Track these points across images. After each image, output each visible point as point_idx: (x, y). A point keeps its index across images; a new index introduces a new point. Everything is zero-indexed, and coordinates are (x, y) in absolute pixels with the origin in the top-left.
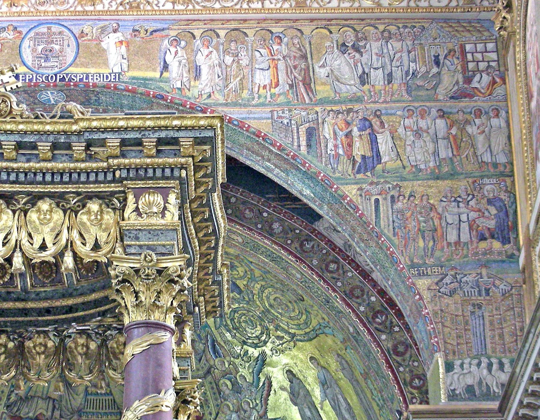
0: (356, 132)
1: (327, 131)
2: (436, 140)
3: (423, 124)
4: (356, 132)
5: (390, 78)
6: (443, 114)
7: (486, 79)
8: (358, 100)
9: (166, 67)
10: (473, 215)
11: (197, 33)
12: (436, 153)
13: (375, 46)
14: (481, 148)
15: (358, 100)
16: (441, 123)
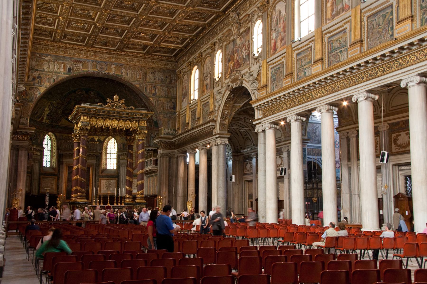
0: (153, 88)
1: (148, 88)
2: (165, 91)
3: (163, 88)
4: (153, 88)
5: (159, 79)
6: (167, 87)
7: (174, 81)
8: (154, 83)
9: (122, 73)
10: (170, 105)
11: (128, 67)
12: (165, 94)
13: (157, 73)
14: (172, 94)
15: (154, 83)
16: (166, 88)
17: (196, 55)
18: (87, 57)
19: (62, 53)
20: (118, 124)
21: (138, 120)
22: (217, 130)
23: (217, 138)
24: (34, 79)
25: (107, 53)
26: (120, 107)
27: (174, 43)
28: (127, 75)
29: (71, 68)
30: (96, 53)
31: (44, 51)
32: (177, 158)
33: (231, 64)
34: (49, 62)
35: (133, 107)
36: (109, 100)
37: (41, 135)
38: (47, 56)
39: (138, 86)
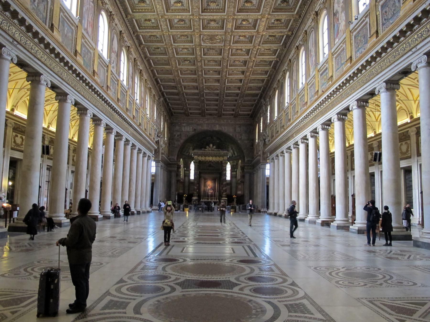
1: (237, 136)
17: (257, 118)
18: (203, 122)
19: (191, 122)
20: (212, 159)
21: (223, 156)
22: (261, 161)
23: (262, 165)
24: (178, 136)
25: (214, 119)
26: (213, 150)
27: (246, 111)
28: (225, 129)
29: (196, 128)
30: (208, 119)
31: (182, 121)
32: (254, 174)
33: (265, 126)
34: (185, 126)
35: (220, 150)
36: (207, 147)
37: (189, 162)
38: (184, 123)
39: (231, 135)
